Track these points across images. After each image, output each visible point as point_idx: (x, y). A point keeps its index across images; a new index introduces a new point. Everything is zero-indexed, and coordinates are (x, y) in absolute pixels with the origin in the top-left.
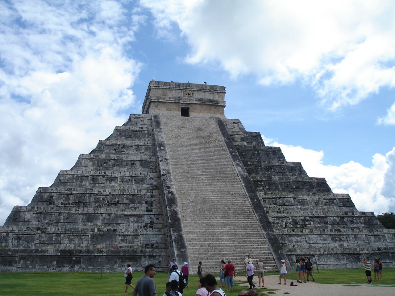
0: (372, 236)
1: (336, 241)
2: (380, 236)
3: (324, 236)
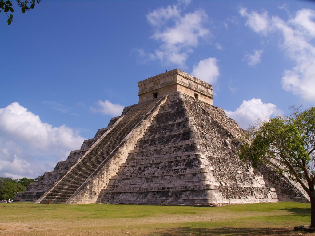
0: (175, 177)
1: (149, 182)
2: (182, 176)
3: (142, 178)
